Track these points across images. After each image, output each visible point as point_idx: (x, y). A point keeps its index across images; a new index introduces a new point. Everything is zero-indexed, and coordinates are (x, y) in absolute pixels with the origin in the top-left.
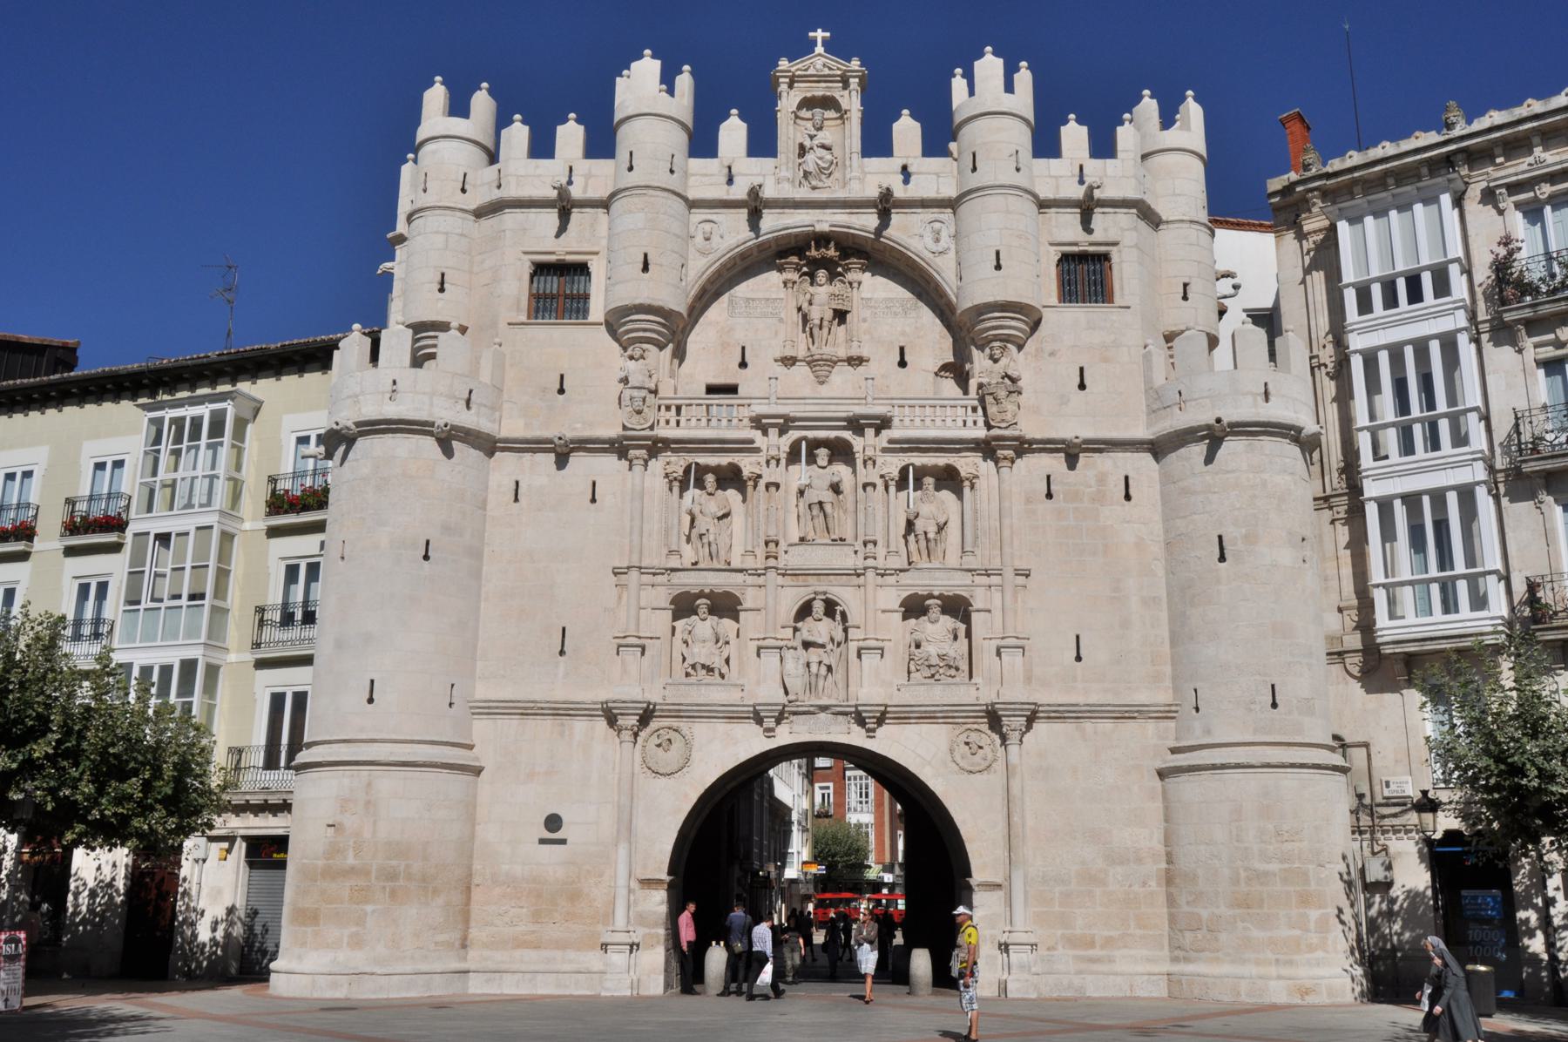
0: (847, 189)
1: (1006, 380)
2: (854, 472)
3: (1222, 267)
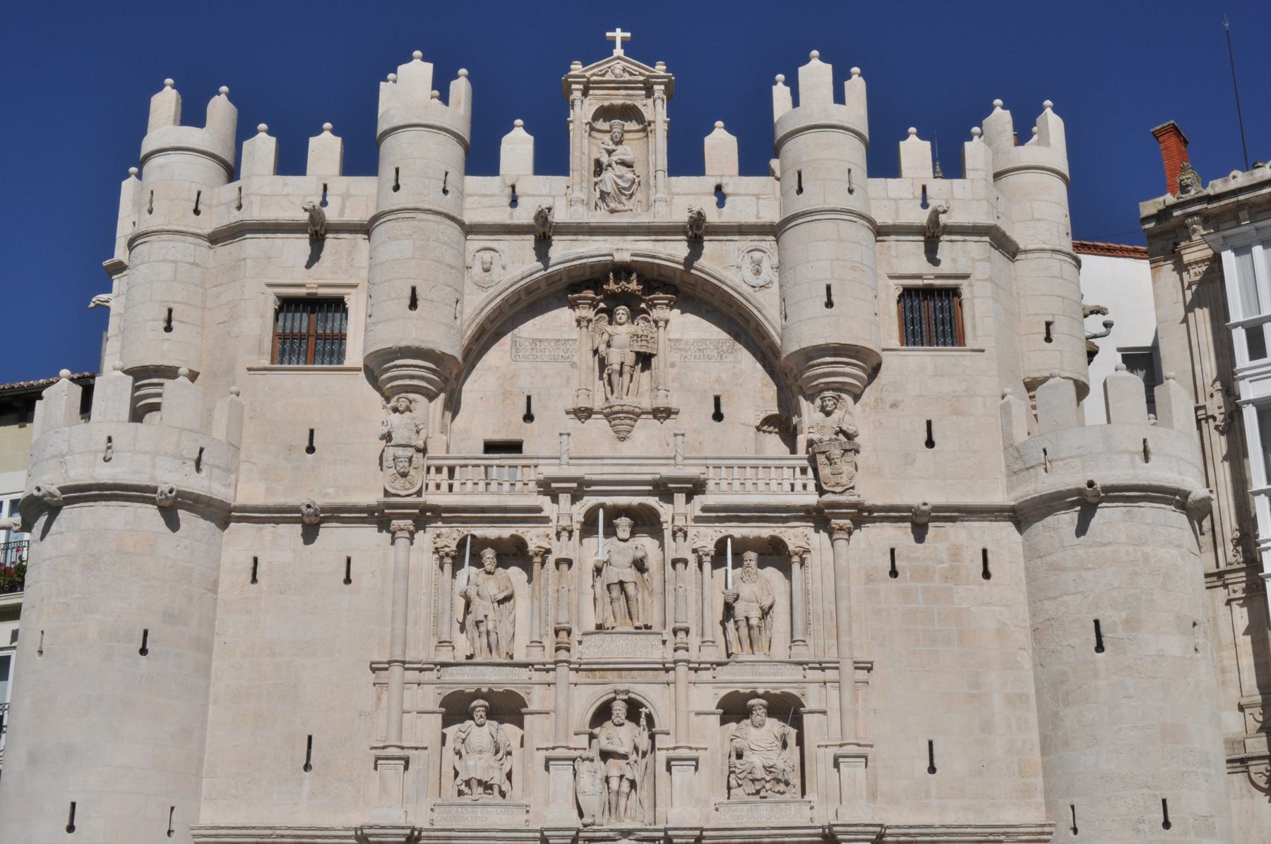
0: (651, 212)
1: (841, 437)
2: (662, 545)
3: (1090, 302)
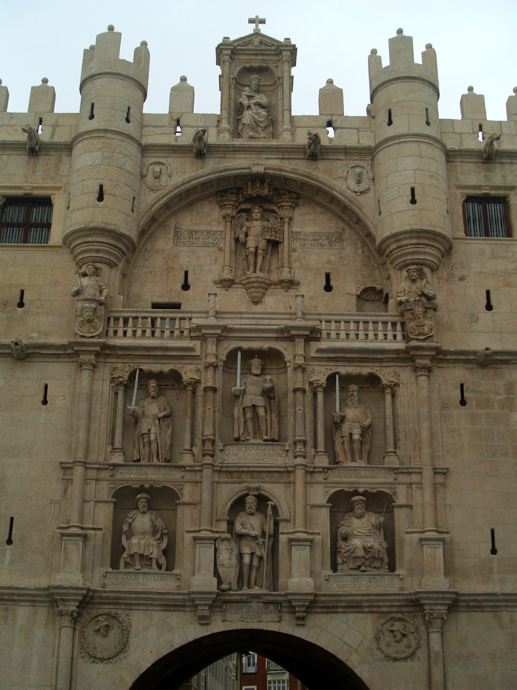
1: (424, 299)
